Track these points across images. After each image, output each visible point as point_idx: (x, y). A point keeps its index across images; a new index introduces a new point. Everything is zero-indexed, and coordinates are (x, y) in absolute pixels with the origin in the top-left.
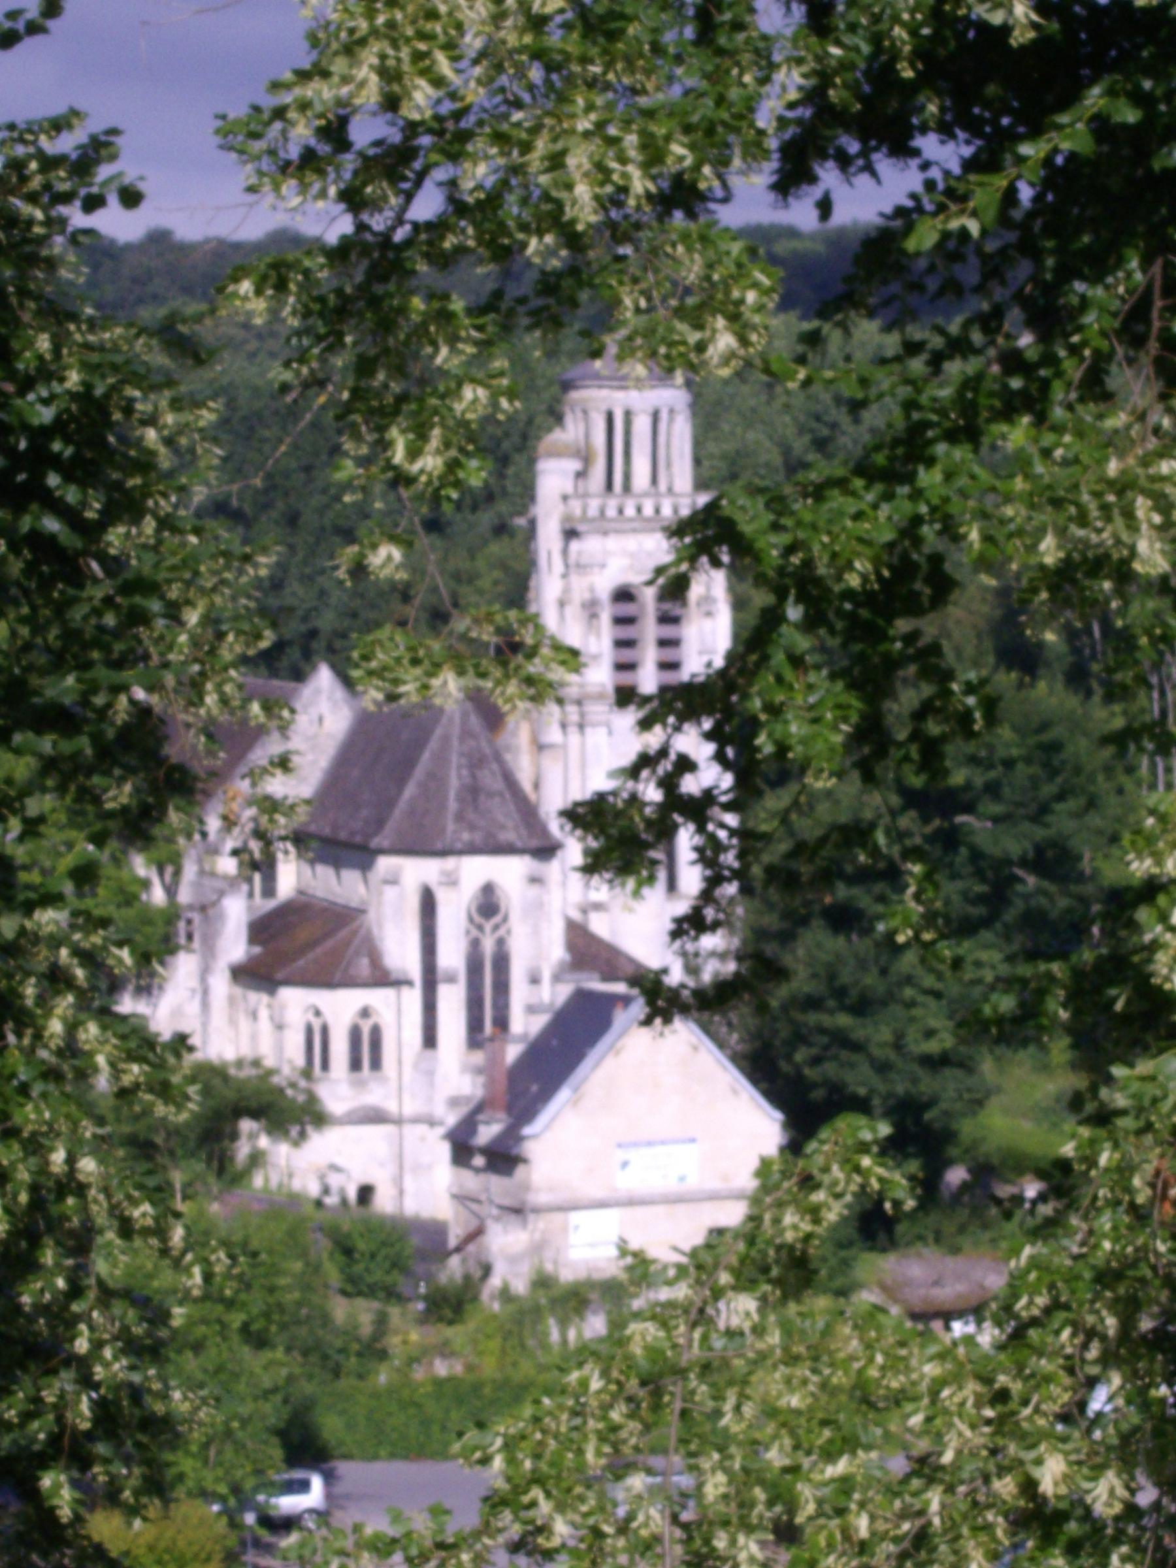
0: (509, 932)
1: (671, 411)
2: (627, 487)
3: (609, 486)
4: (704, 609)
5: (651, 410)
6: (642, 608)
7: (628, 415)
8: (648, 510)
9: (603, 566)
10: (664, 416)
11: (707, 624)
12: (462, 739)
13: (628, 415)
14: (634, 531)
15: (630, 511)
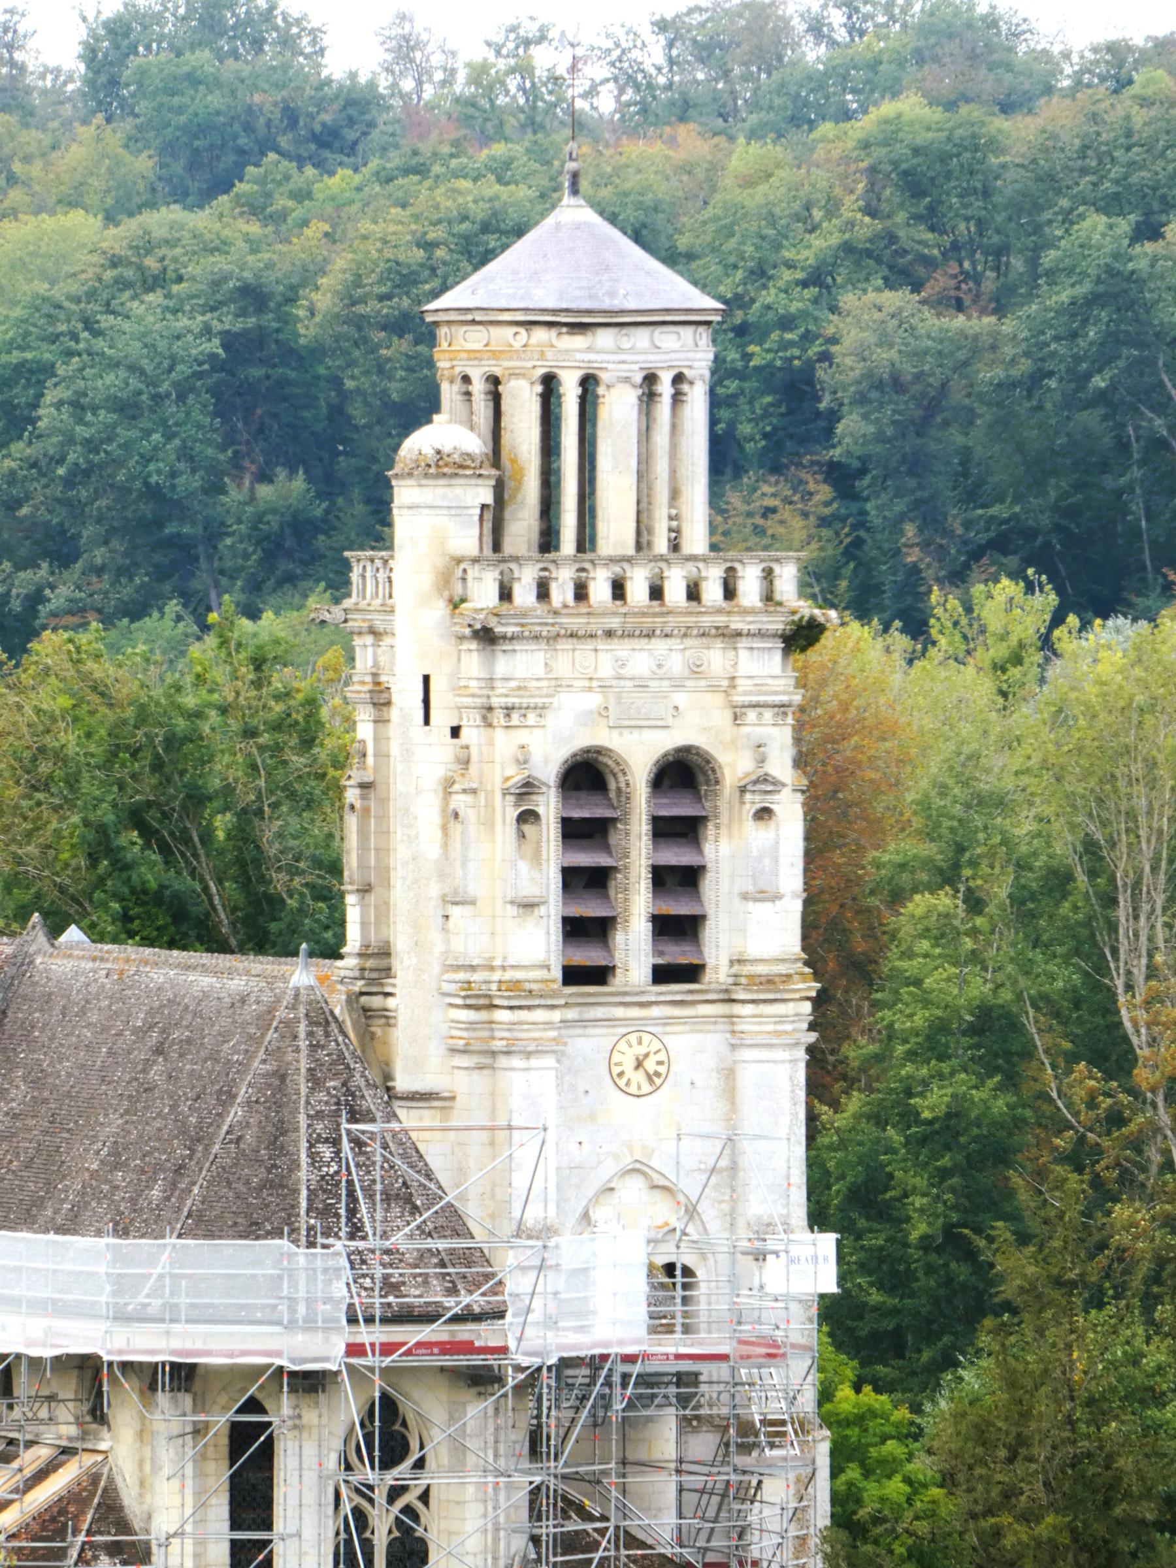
0: (425, 1497)
1: (678, 379)
2: (586, 541)
3: (548, 541)
4: (753, 802)
5: (638, 378)
6: (625, 796)
7: (588, 383)
8: (637, 591)
9: (541, 709)
10: (665, 388)
11: (756, 835)
12: (316, 1082)
13: (588, 383)
14: (609, 634)
15: (600, 591)
